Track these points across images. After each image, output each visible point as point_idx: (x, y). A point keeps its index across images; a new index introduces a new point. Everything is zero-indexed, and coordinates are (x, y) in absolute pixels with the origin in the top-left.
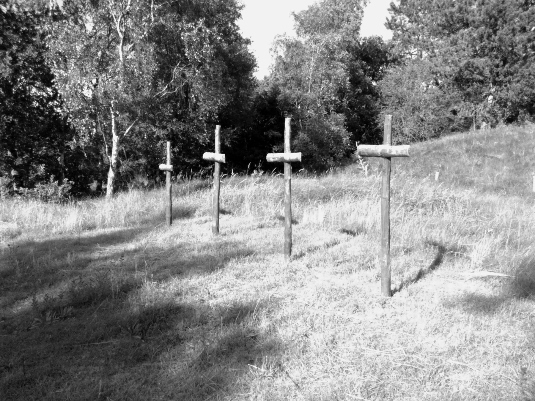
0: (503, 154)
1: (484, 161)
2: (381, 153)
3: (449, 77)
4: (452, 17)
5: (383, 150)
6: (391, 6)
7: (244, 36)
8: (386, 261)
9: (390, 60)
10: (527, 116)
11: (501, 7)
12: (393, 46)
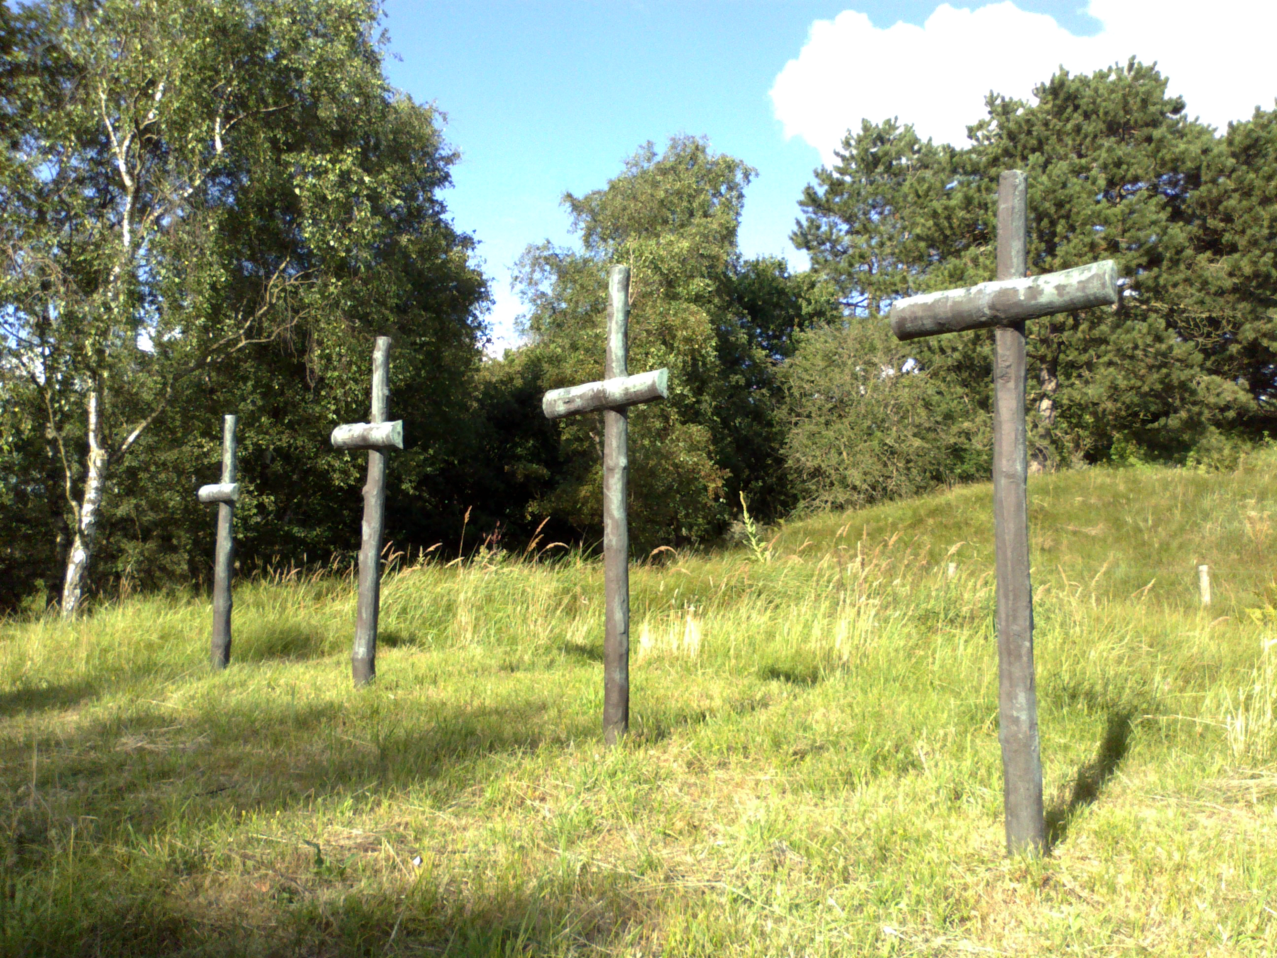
0: (1101, 525)
1: (1057, 542)
2: (992, 307)
3: (949, 352)
4: (949, 218)
5: (1003, 292)
6: (808, 194)
7: (459, 229)
8: (1024, 717)
9: (808, 313)
10: (1131, 448)
11: (1061, 194)
12: (813, 285)
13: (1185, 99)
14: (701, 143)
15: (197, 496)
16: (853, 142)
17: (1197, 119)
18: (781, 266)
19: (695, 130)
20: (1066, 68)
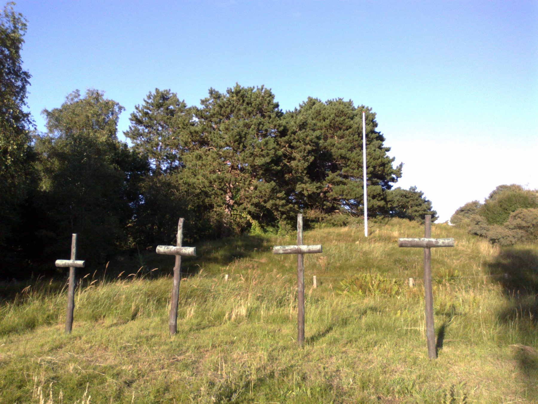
2: (427, 244)
5: (429, 241)
13: (279, 104)
14: (100, 92)
15: (54, 264)
16: (152, 98)
18: (126, 146)
19: (99, 88)
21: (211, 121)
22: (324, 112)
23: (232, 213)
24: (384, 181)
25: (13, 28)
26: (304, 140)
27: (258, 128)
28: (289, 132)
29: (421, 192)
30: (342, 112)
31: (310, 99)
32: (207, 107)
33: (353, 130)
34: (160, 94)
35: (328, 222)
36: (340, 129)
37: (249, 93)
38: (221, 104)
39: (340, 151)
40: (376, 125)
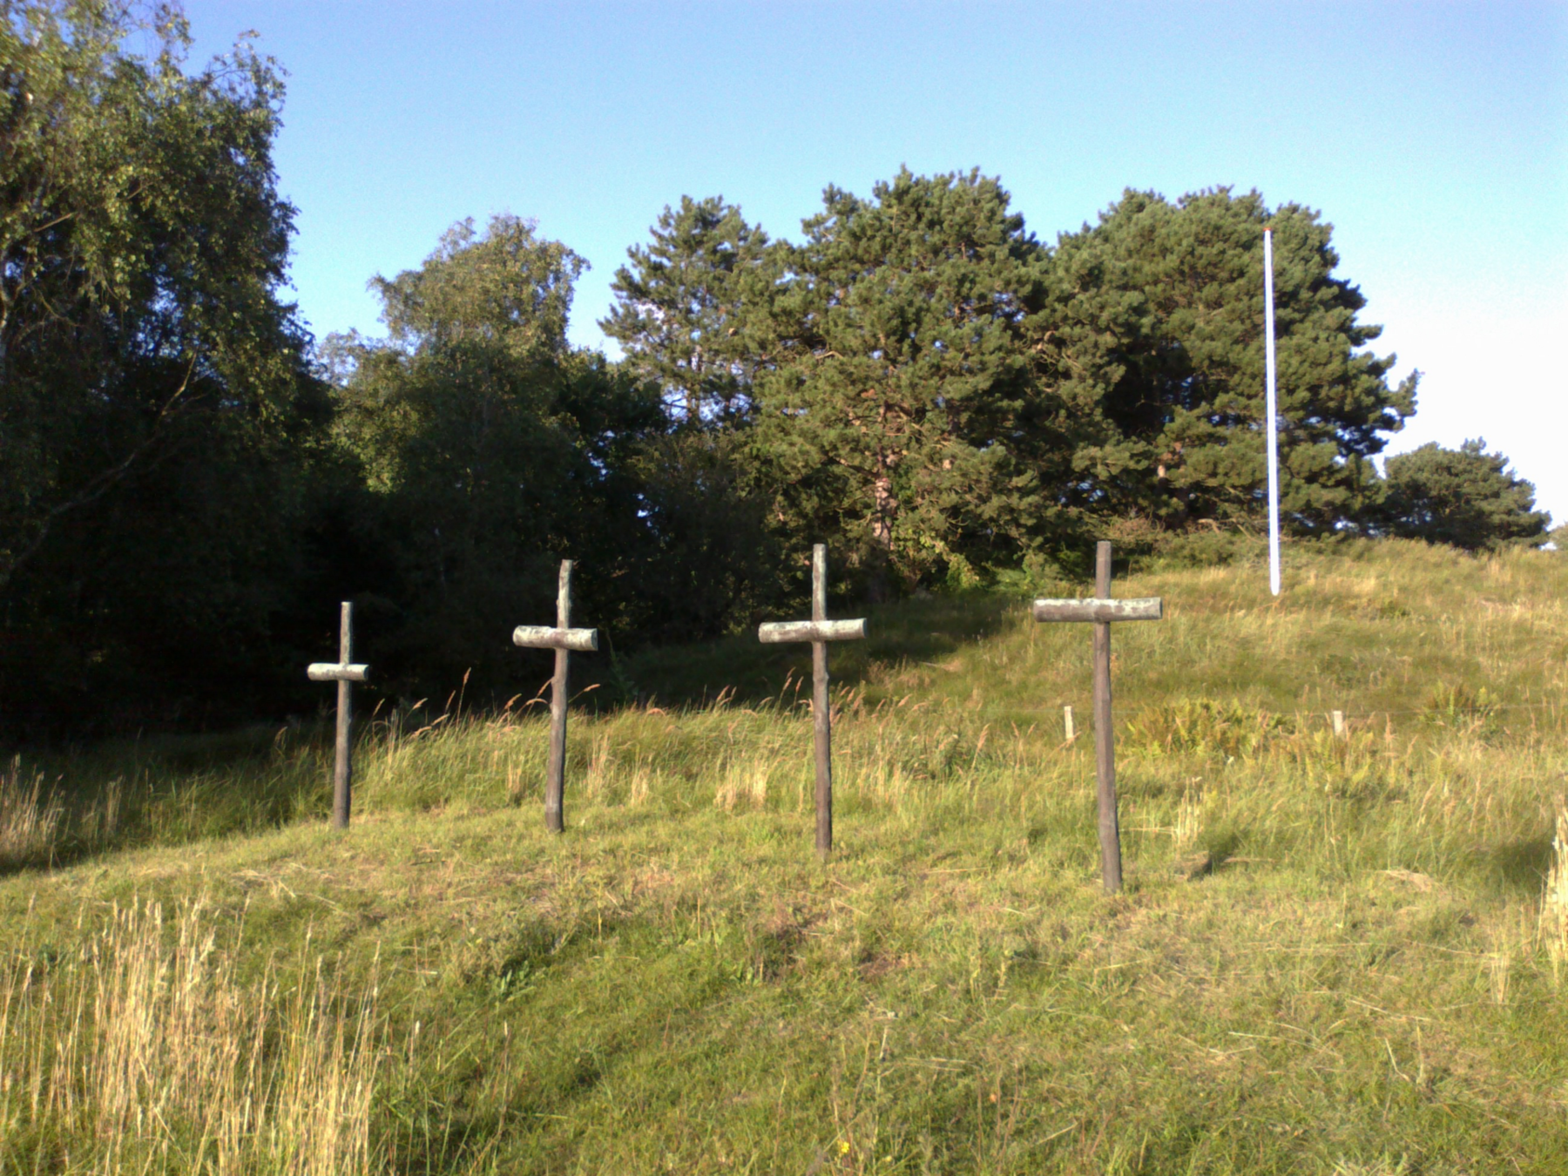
5: (1103, 606)
13: (1026, 217)
16: (672, 222)
17: (1033, 235)
18: (601, 360)
20: (910, 168)
21: (827, 279)
22: (1164, 231)
23: (894, 534)
24: (1359, 429)
25: (254, 96)
26: (1094, 319)
27: (958, 293)
28: (1050, 299)
29: (1498, 456)
30: (1218, 228)
31: (1130, 195)
32: (818, 240)
33: (1249, 282)
34: (694, 211)
35: (1174, 554)
36: (1213, 278)
37: (937, 192)
38: (857, 230)
39: (1208, 346)
40: (1330, 261)
